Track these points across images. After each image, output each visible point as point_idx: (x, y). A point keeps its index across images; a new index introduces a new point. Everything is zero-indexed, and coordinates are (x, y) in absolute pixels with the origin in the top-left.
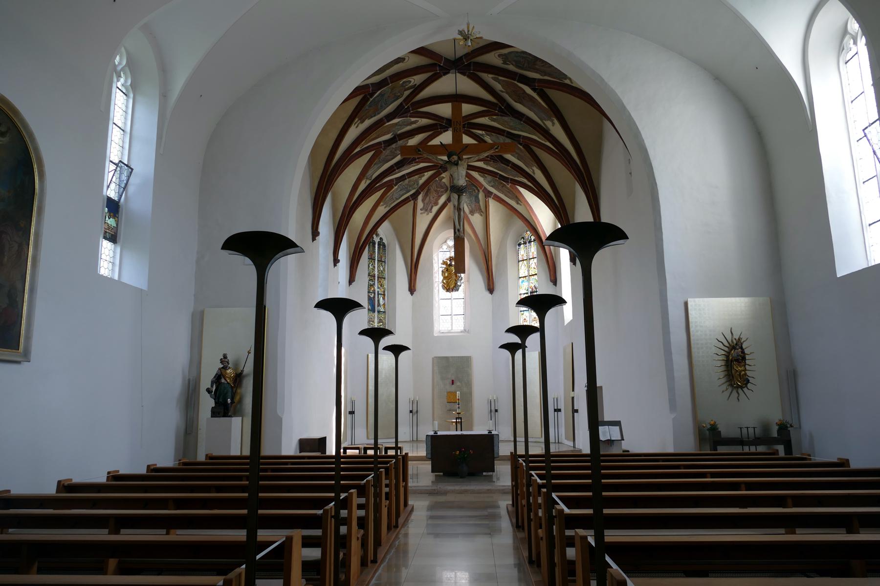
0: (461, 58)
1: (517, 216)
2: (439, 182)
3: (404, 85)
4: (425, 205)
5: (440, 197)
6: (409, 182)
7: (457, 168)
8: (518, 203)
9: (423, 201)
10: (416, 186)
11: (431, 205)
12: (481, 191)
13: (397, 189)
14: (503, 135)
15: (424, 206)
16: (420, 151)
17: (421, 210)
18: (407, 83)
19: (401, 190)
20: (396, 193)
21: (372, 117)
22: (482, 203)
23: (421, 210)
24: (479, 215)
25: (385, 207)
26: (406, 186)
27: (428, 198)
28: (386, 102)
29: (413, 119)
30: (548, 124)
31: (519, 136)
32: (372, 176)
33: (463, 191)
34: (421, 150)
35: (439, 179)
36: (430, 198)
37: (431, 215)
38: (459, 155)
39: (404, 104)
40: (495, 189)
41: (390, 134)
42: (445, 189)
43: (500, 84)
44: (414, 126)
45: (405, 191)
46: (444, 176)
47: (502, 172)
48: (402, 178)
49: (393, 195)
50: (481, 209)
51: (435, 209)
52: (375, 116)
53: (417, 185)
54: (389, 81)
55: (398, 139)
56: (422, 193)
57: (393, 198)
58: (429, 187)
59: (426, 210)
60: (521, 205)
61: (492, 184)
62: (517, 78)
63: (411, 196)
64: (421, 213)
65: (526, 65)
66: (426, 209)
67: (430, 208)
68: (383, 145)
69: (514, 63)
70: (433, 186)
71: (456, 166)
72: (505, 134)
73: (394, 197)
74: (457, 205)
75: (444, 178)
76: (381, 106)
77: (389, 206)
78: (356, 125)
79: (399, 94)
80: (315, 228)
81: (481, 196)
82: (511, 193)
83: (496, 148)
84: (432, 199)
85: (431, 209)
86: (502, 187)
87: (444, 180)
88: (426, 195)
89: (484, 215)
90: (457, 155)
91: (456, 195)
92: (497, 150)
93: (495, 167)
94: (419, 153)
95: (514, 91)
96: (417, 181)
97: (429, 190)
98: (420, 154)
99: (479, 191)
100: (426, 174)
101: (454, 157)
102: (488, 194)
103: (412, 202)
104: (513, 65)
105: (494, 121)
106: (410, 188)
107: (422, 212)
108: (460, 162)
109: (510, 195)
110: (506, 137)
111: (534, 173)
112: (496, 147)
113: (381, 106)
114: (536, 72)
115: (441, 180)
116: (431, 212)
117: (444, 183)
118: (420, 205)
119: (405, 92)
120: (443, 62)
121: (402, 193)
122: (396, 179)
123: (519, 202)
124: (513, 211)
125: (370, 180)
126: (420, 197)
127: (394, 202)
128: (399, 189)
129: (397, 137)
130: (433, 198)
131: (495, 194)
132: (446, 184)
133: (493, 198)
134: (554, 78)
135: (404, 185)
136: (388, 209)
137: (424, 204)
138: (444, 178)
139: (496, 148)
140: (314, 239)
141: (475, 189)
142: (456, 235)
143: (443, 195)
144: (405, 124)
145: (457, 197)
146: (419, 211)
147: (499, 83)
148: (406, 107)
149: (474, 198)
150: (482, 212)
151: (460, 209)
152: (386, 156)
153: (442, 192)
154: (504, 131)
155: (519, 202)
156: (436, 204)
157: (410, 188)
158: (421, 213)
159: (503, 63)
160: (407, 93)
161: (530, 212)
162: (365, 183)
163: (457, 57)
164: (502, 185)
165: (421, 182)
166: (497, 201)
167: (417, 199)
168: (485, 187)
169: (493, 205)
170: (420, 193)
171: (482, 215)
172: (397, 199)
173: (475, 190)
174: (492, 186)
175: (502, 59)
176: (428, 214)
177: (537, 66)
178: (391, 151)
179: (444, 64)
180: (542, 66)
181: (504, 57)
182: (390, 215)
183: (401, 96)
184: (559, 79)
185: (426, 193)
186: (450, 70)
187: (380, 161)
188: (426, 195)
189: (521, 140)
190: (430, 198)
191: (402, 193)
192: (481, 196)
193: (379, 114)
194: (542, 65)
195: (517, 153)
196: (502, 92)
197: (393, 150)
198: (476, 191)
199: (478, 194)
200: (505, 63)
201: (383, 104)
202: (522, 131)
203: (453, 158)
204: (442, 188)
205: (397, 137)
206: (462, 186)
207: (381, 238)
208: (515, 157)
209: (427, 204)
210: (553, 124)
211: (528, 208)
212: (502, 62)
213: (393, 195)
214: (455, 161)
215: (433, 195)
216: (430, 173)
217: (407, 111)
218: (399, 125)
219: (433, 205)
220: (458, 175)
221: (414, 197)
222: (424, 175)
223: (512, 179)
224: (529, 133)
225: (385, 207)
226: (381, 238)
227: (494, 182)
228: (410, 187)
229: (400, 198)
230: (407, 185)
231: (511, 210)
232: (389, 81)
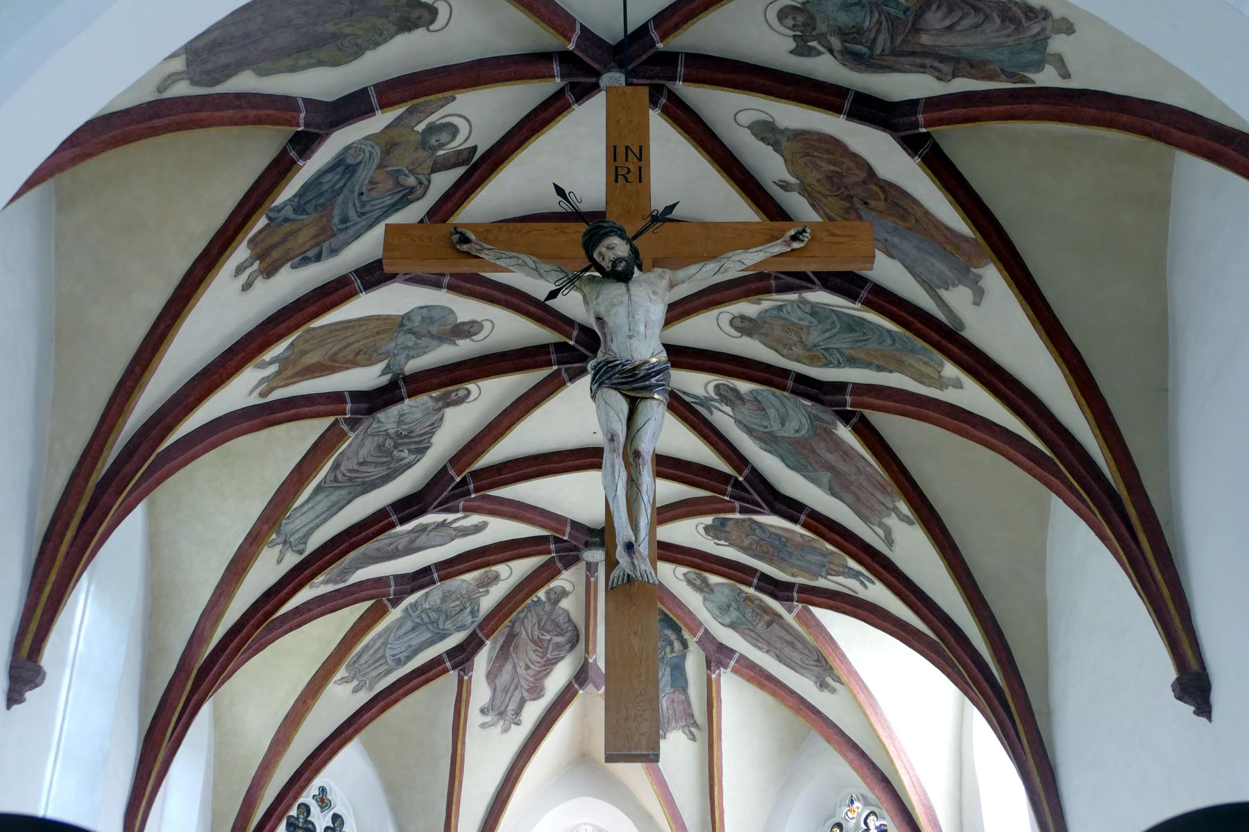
0: (644, 29)
1: (821, 733)
2: (548, 607)
3: (433, 141)
4: (498, 693)
5: (550, 664)
6: (443, 600)
7: (628, 290)
8: (823, 685)
9: (491, 676)
10: (466, 618)
11: (517, 695)
12: (692, 642)
13: (400, 622)
14: (784, 388)
15: (493, 699)
16: (466, 240)
17: (483, 711)
18: (444, 137)
19: (413, 629)
20: (399, 638)
21: (305, 261)
22: (695, 691)
23: (483, 711)
24: (684, 737)
25: (355, 691)
26: (433, 615)
27: (508, 667)
28: (363, 204)
29: (475, 519)
30: (958, 298)
31: (840, 387)
32: (304, 540)
33: (653, 381)
34: (473, 237)
35: (549, 598)
36: (515, 667)
37: (519, 735)
38: (635, 242)
39: (452, 472)
40: (744, 635)
41: (381, 366)
42: (568, 634)
43: (782, 155)
44: (463, 349)
45: (427, 635)
46: (568, 587)
47: (770, 561)
48: (421, 578)
49: (385, 644)
50: (692, 716)
51: (533, 711)
52: (318, 258)
53: (474, 613)
54: (374, 101)
55: (404, 390)
56: (488, 643)
57: (383, 657)
58: (512, 627)
59: (501, 714)
60: (833, 691)
61: (734, 614)
62: (847, 106)
63: (452, 653)
64: (483, 726)
65: (882, 42)
66: (502, 711)
67: (512, 706)
68: (349, 406)
69: (836, 43)
70: (528, 626)
71: (623, 285)
72: (790, 383)
73: (389, 653)
74: (622, 438)
75: (564, 593)
76: (344, 220)
77: (370, 689)
78: (244, 277)
79: (411, 181)
80: (25, 651)
81: (693, 663)
82: (799, 646)
83: (794, 238)
84: (521, 671)
85: (518, 712)
86: (769, 624)
87: (565, 604)
88: (504, 654)
89: (702, 736)
90: (629, 241)
91: (619, 397)
92: (796, 245)
93: (747, 543)
94: (465, 247)
95: (829, 178)
96: (471, 601)
97: (512, 637)
98: (468, 254)
99: (685, 645)
100: (502, 569)
101: (615, 240)
102: (718, 655)
103: (453, 675)
104: (831, 51)
105: (750, 335)
106: (449, 625)
107: (488, 719)
108: (637, 272)
109: (796, 656)
110: (794, 392)
111: (889, 541)
112: (792, 232)
113: (344, 220)
114: (922, 69)
115: (557, 601)
116: (517, 724)
117: (566, 612)
118: (480, 692)
119: (433, 176)
120: (575, 38)
121: (416, 639)
122: (399, 578)
123: (829, 680)
124: (805, 717)
125: (300, 552)
126: (482, 661)
127: (388, 672)
128: (408, 625)
129: (401, 383)
130: (527, 667)
131: (741, 656)
132: (573, 616)
133: (735, 671)
134: (989, 77)
135: (424, 611)
136: (364, 697)
137: (494, 690)
138: (564, 593)
139: (794, 238)
140: (14, 697)
141: (673, 637)
142: (615, 573)
143: (563, 658)
144: (434, 329)
145: (624, 407)
146: (474, 718)
147: (777, 147)
148: (458, 479)
149: (668, 669)
150: (695, 724)
151: (637, 454)
152: (361, 464)
153: (558, 646)
154: (785, 373)
155: (829, 680)
156: (536, 691)
157: (449, 625)
158: (483, 726)
159: (791, 52)
160: (443, 181)
161: (869, 711)
162: (279, 561)
163: (630, 30)
164: (767, 618)
165: (487, 603)
166: (750, 680)
167: (471, 669)
168: (706, 631)
169: (731, 687)
170: (481, 644)
171: (694, 738)
172: (400, 663)
173: (671, 644)
174: (732, 626)
175: (794, 27)
176: (506, 730)
177: (925, 39)
178: (380, 447)
179: (577, 46)
180: (950, 28)
181: (800, 19)
182: (372, 719)
183: (419, 191)
184: (1011, 76)
185: (502, 647)
186: (598, 75)
187: (336, 480)
188: (504, 654)
189: (848, 398)
190: (515, 667)
191: (416, 639)
192: (693, 663)
193: (334, 252)
194: (947, 23)
195: (830, 468)
196: (785, 186)
197: (390, 443)
198: (677, 645)
199: (683, 658)
200: (802, 49)
201: (352, 214)
202: (852, 362)
203: (610, 248)
204: (561, 635)
205: (401, 383)
206: (645, 362)
207: (336, 818)
208: (820, 486)
209: (506, 690)
210: (979, 294)
211: (861, 697)
212: (792, 44)
213: (385, 644)
214: (615, 263)
215: (527, 655)
216: (522, 567)
217: (461, 490)
218: (410, 331)
219: (526, 694)
220: (631, 315)
221: (462, 656)
222: (496, 578)
223: (804, 589)
224: (879, 369)
225: (355, 691)
226: (336, 818)
227: (738, 610)
228: (447, 618)
229: (409, 658)
230: (438, 610)
231: (798, 711)
232: (374, 101)
